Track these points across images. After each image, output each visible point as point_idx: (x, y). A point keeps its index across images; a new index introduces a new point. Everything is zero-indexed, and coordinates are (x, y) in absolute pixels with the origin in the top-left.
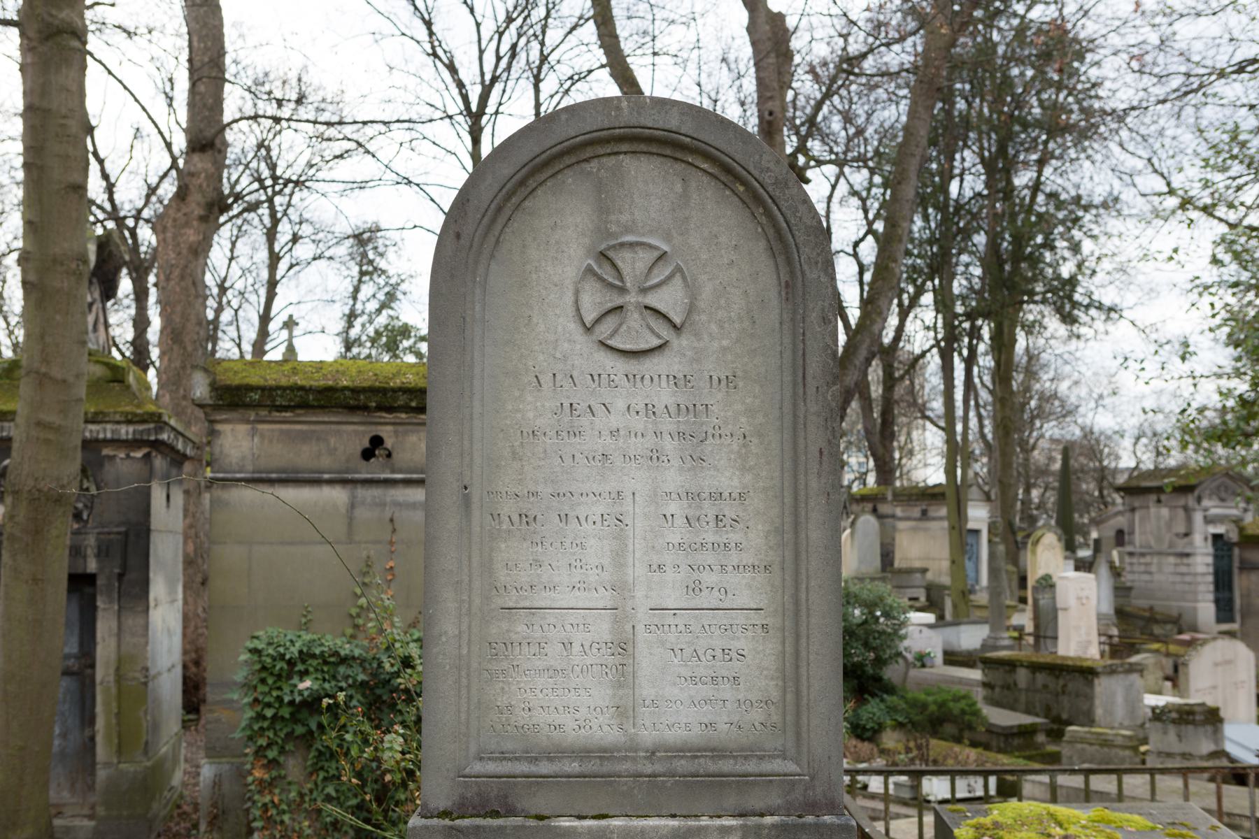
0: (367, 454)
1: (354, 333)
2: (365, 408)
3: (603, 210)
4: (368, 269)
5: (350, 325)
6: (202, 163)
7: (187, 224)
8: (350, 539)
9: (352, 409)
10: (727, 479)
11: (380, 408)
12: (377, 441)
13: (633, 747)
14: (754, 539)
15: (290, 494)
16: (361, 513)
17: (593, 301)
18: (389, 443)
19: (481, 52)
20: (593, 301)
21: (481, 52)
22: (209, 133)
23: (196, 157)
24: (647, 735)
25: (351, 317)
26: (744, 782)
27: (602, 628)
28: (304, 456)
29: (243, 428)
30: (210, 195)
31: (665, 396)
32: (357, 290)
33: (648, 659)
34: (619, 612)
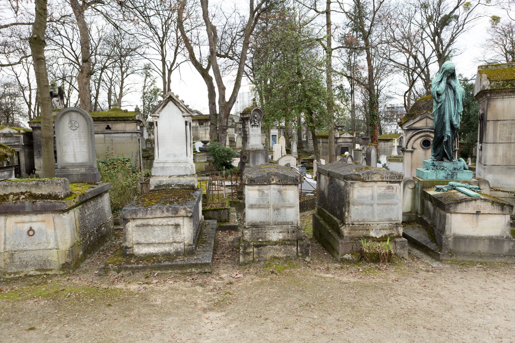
1: (145, 91)
2: (105, 121)
3: (70, 117)
4: (148, 75)
5: (144, 89)
6: (86, 65)
7: (84, 78)
8: (105, 143)
10: (83, 140)
11: (108, 120)
12: (108, 126)
13: (76, 163)
14: (85, 145)
16: (106, 138)
18: (110, 127)
20: (70, 125)
22: (86, 58)
23: (84, 63)
24: (77, 162)
25: (144, 87)
26: (85, 165)
27: (73, 153)
30: (88, 72)
32: (145, 80)
33: (77, 156)
34: (74, 152)
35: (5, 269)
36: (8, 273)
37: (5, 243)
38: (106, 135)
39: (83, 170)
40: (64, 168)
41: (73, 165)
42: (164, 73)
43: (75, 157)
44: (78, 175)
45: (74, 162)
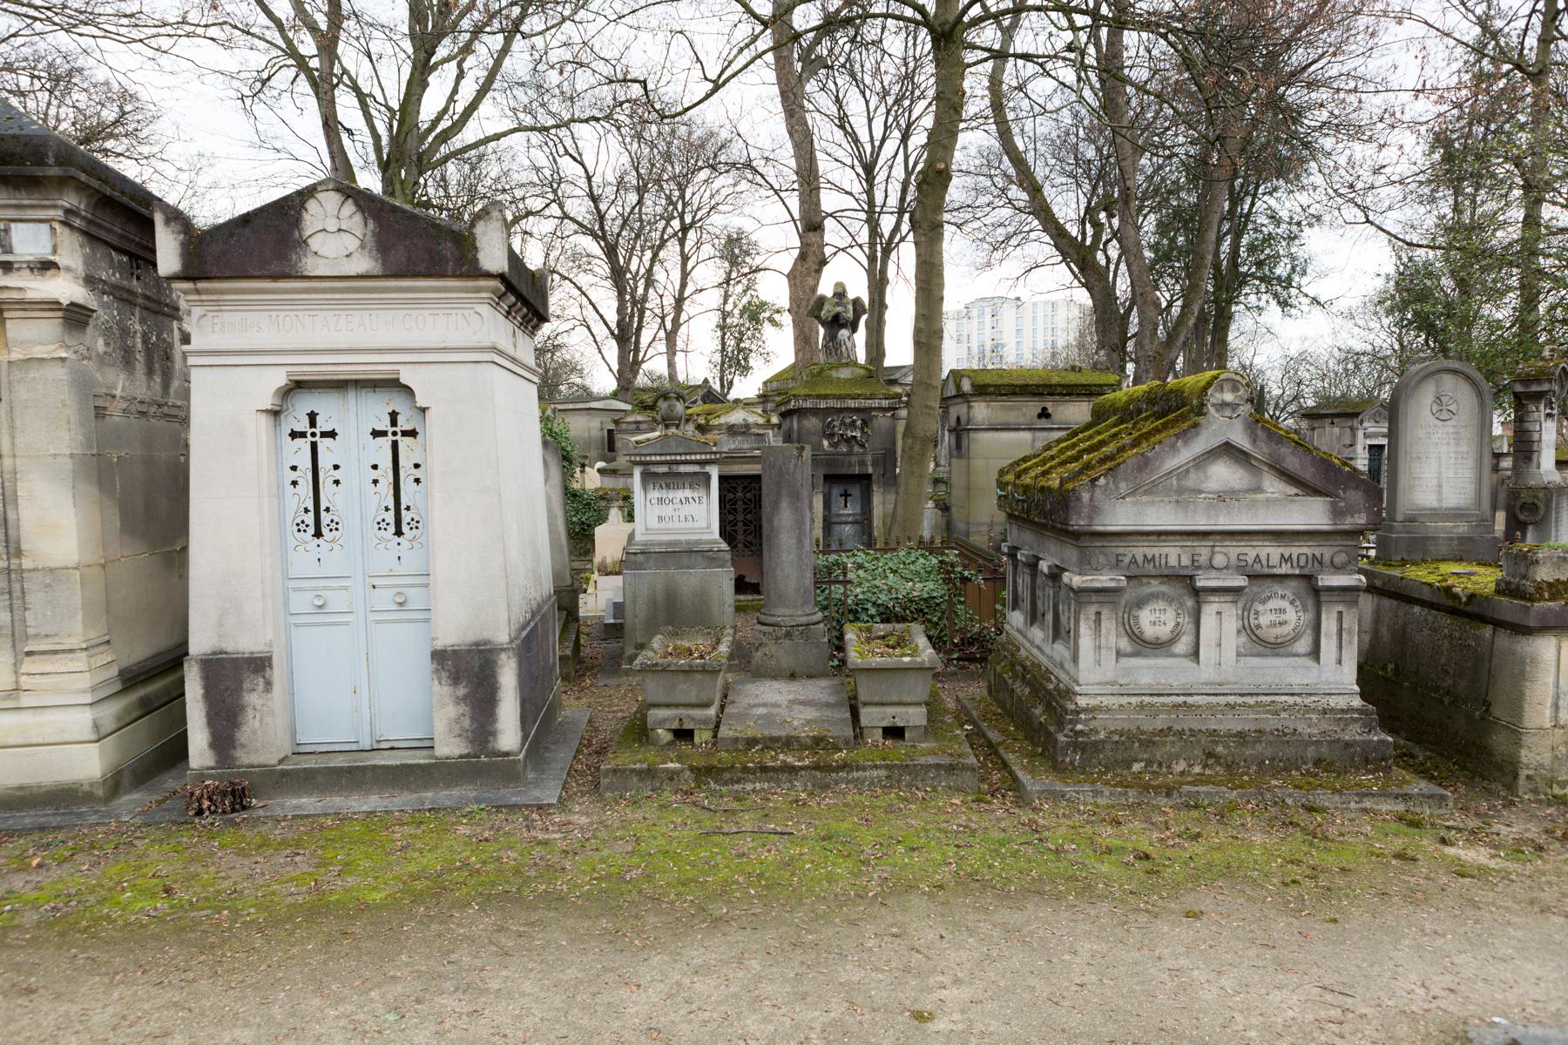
0: (1040, 416)
1: (729, 307)
2: (1042, 394)
3: (1438, 387)
9: (1035, 395)
10: (1465, 449)
12: (1044, 409)
14: (1470, 462)
15: (996, 435)
17: (1435, 408)
18: (1050, 411)
19: (870, 121)
20: (1435, 408)
21: (870, 121)
28: (1012, 417)
29: (983, 404)
31: (1451, 430)
34: (1439, 479)
35: (1552, 770)
36: (1558, 783)
37: (1556, 707)
38: (1038, 434)
39: (1462, 528)
40: (1411, 519)
41: (1436, 514)
42: (872, 258)
43: (1440, 493)
44: (1451, 539)
45: (1435, 504)
